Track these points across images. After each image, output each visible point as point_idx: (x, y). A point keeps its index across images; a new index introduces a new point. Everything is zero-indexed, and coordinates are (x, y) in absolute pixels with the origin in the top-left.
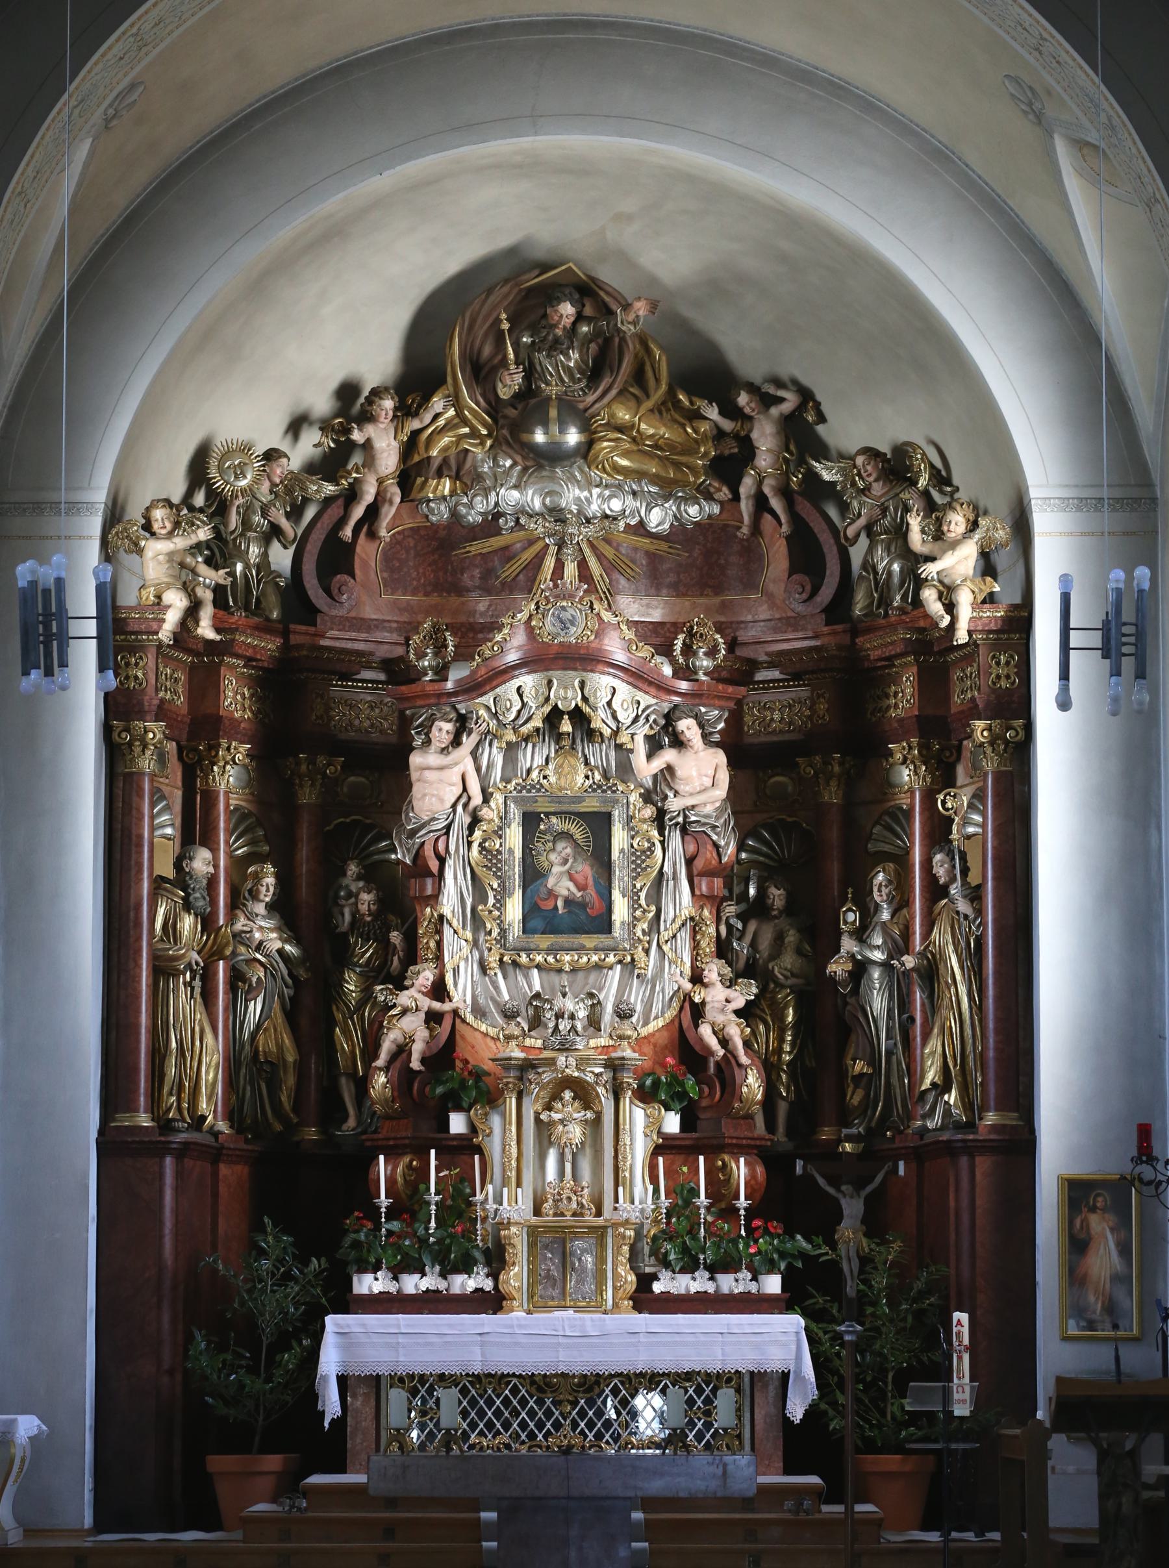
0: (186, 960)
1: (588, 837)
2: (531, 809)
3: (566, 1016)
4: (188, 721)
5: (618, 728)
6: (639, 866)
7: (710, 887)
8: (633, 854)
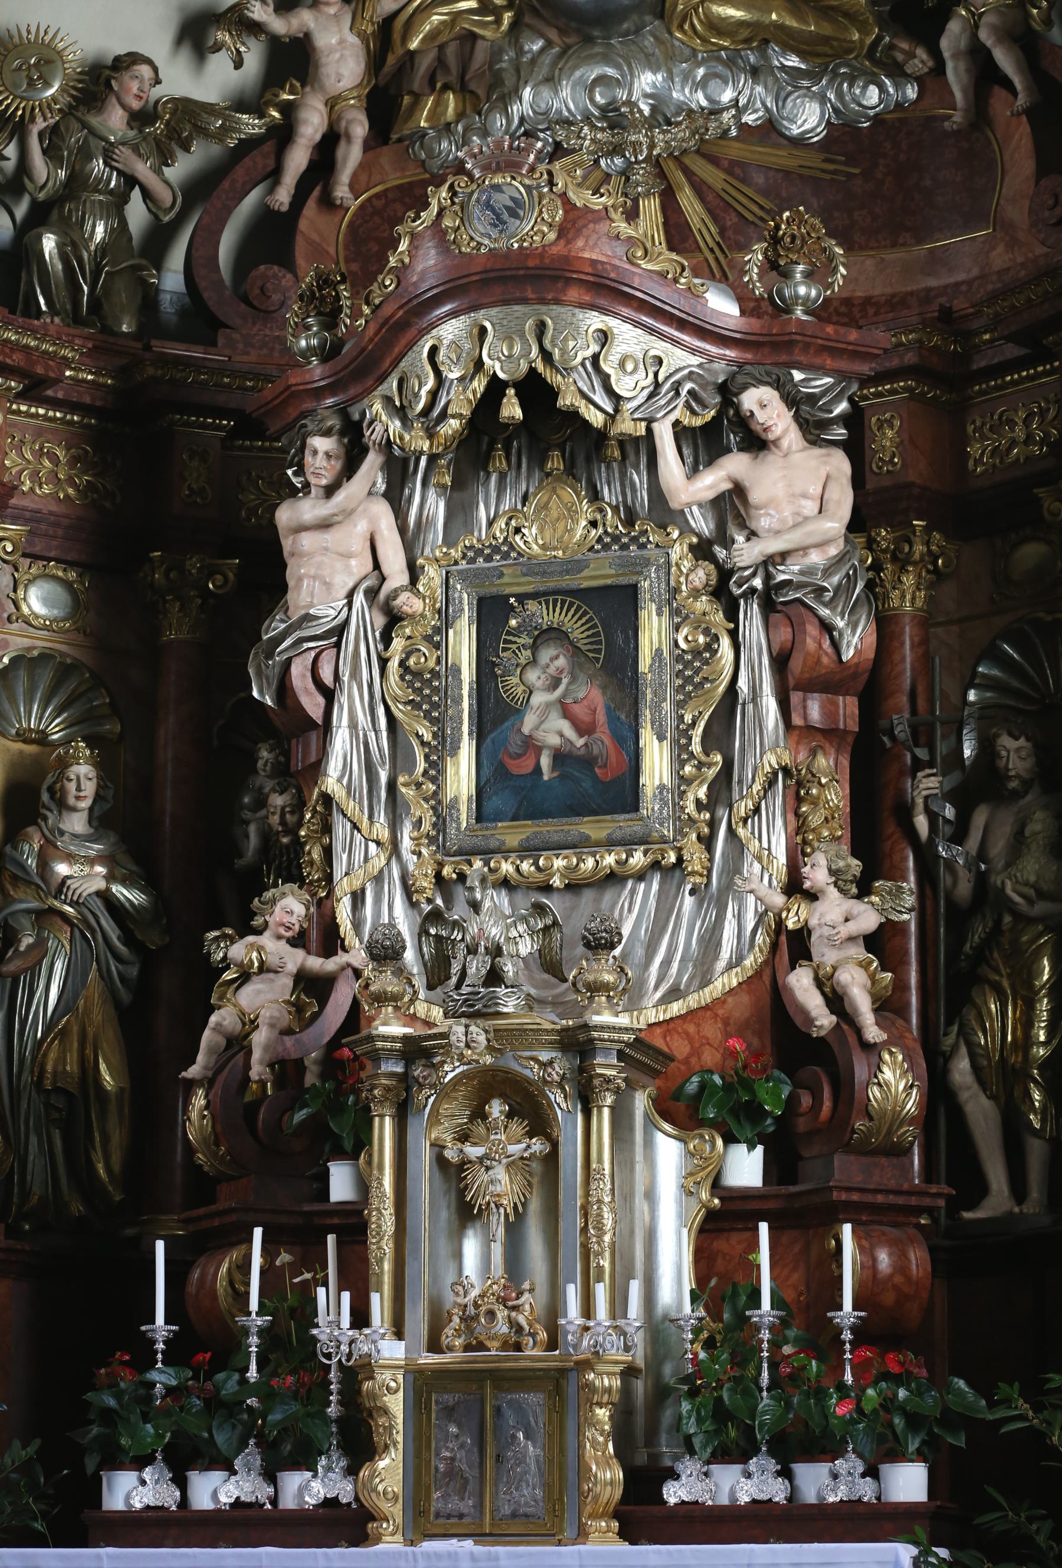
1: (597, 634)
2: (494, 590)
3: (481, 949)
5: (617, 410)
6: (688, 680)
7: (830, 713)
8: (679, 659)
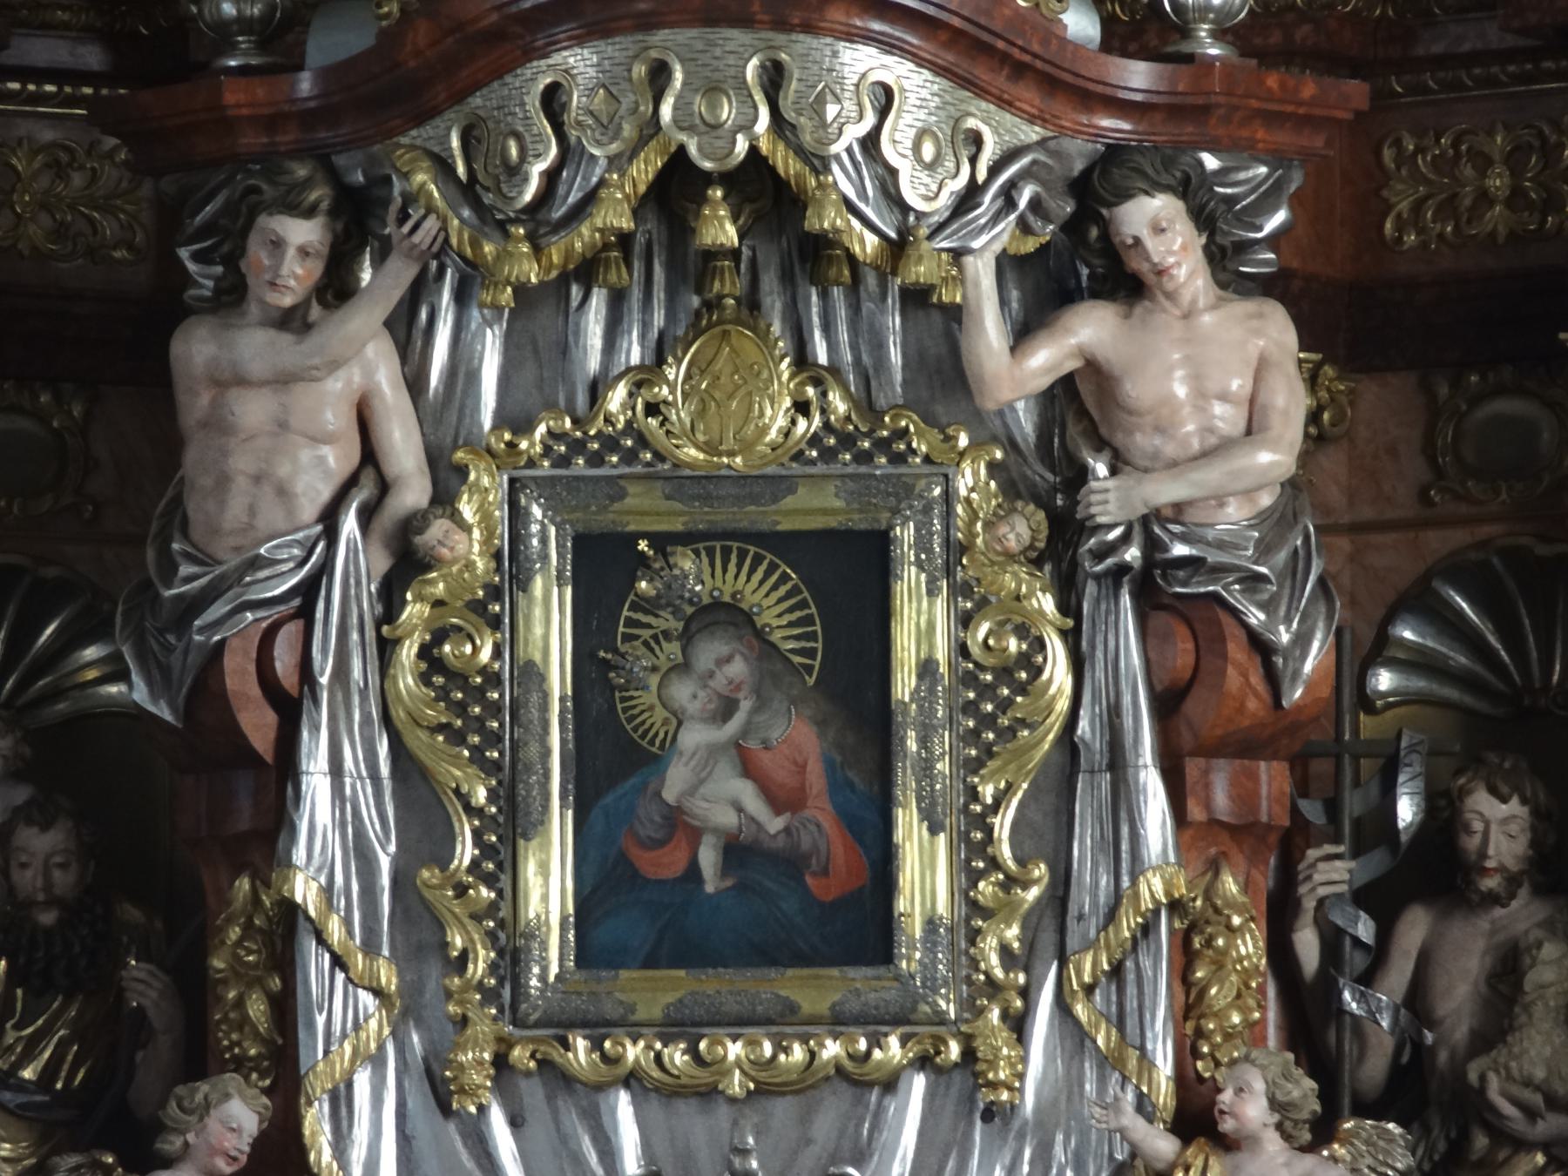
6: (989, 721)
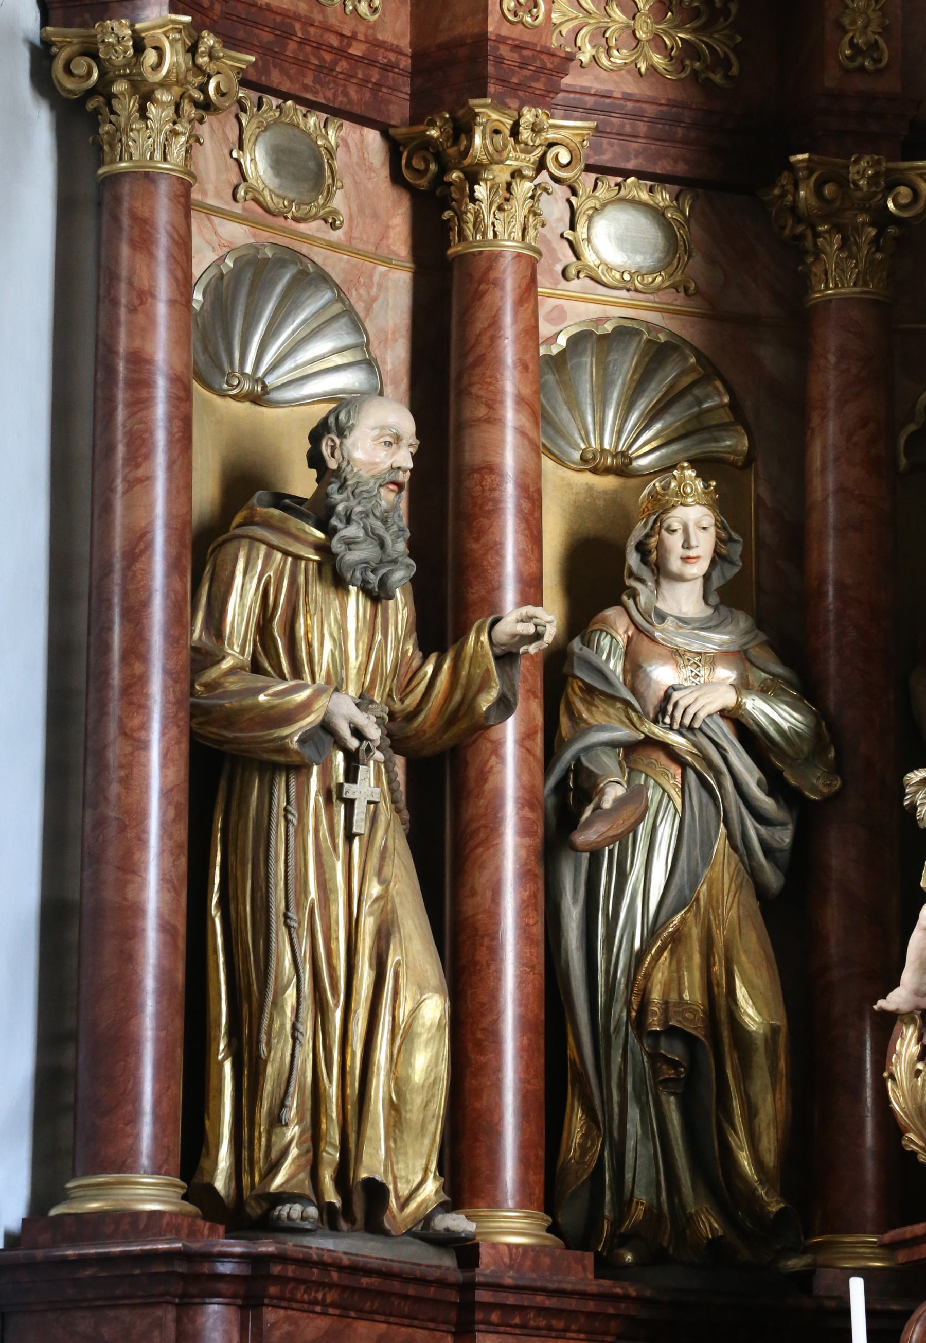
0: (310, 720)
4: (405, 63)
